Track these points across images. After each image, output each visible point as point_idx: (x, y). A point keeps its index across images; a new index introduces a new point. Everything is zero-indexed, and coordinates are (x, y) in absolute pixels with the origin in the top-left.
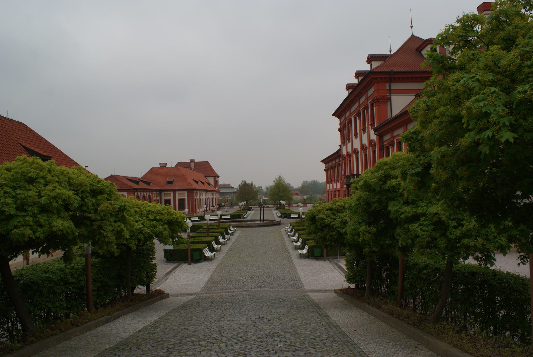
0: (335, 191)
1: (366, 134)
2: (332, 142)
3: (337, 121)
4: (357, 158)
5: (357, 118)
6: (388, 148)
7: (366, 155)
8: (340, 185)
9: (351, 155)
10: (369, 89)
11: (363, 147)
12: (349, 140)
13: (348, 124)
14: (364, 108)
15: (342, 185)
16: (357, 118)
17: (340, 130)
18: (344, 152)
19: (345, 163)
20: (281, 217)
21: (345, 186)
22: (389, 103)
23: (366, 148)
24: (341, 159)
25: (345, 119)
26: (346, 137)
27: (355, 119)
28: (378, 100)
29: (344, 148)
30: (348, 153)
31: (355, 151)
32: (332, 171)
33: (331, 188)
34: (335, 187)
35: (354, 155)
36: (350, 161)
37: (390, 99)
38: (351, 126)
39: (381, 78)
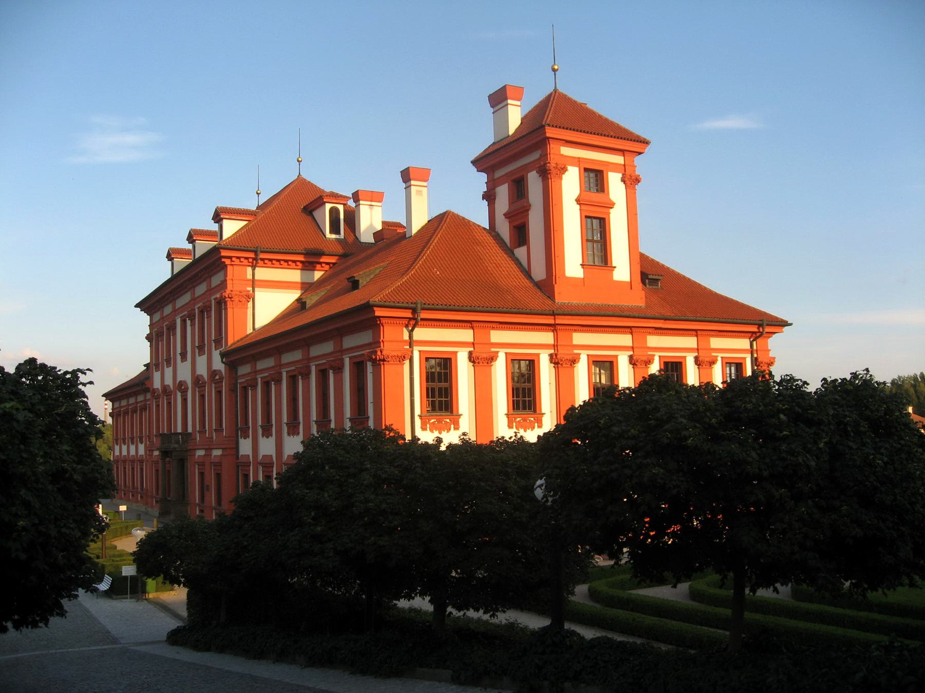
1: (205, 357)
3: (144, 319)
4: (185, 400)
5: (188, 322)
6: (245, 389)
7: (202, 396)
11: (197, 381)
13: (168, 329)
15: (149, 450)
16: (188, 322)
17: (149, 338)
18: (157, 384)
19: (158, 406)
21: (156, 453)
24: (149, 396)
27: (184, 322)
29: (157, 376)
30: (165, 388)
31: (181, 387)
35: (179, 394)
36: (169, 403)
38: (175, 334)
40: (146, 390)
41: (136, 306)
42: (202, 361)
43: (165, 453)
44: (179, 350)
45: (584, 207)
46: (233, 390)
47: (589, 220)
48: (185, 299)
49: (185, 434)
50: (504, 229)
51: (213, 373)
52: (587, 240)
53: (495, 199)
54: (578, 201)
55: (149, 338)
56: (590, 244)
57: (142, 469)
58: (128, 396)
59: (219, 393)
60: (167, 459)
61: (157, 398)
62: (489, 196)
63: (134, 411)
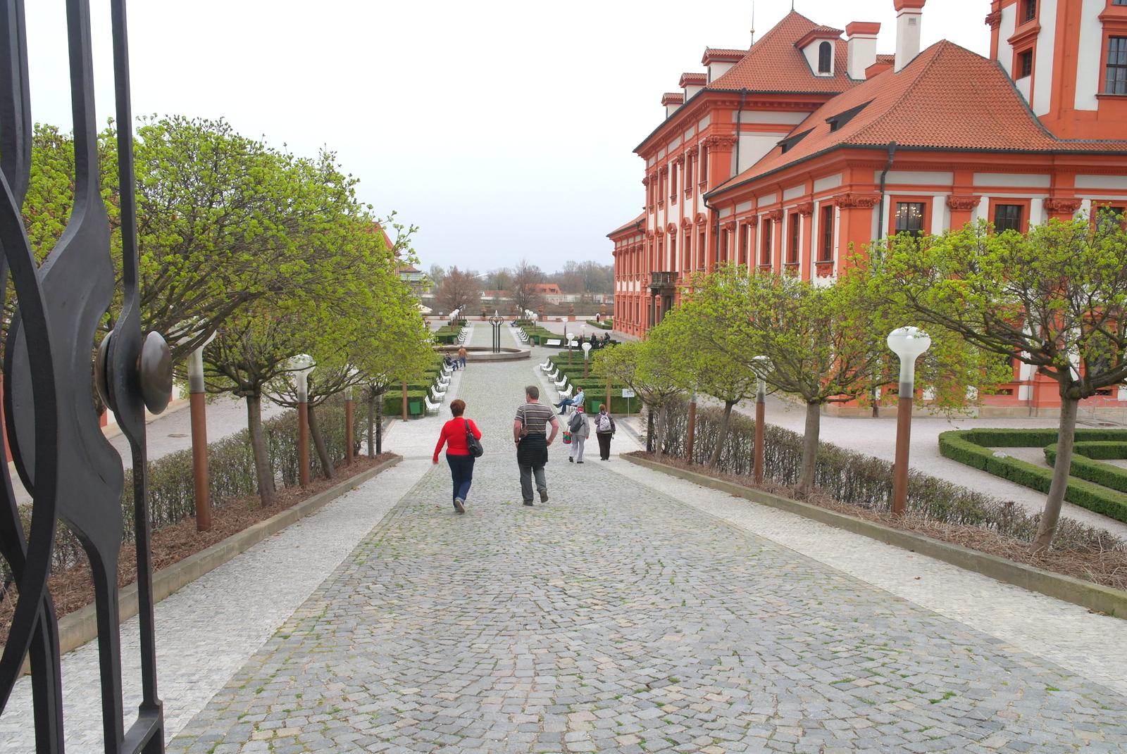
0: (631, 297)
2: (630, 202)
3: (640, 165)
4: (674, 242)
5: (678, 166)
6: (725, 231)
7: (688, 238)
8: (642, 288)
9: (662, 234)
10: (701, 119)
11: (684, 223)
12: (661, 204)
14: (691, 151)
17: (645, 182)
18: (651, 227)
19: (652, 246)
20: (528, 343)
21: (649, 290)
22: (734, 150)
23: (690, 226)
24: (644, 235)
25: (657, 163)
26: (656, 199)
27: (675, 166)
28: (715, 142)
29: (651, 217)
31: (670, 228)
32: (628, 257)
33: (624, 289)
34: (631, 289)
35: (669, 236)
36: (661, 244)
37: (737, 142)
39: (724, 102)
40: (643, 232)
41: (635, 151)
42: (689, 204)
43: (655, 292)
44: (670, 195)
45: (1108, 26)
46: (714, 232)
47: (1114, 41)
48: (675, 144)
49: (673, 275)
50: (1007, 58)
51: (698, 217)
52: (1108, 66)
53: (999, 22)
54: (1103, 19)
55: (645, 182)
56: (1111, 70)
57: (638, 304)
58: (627, 237)
59: (703, 235)
60: (657, 296)
61: (652, 238)
62: (994, 20)
63: (633, 250)
